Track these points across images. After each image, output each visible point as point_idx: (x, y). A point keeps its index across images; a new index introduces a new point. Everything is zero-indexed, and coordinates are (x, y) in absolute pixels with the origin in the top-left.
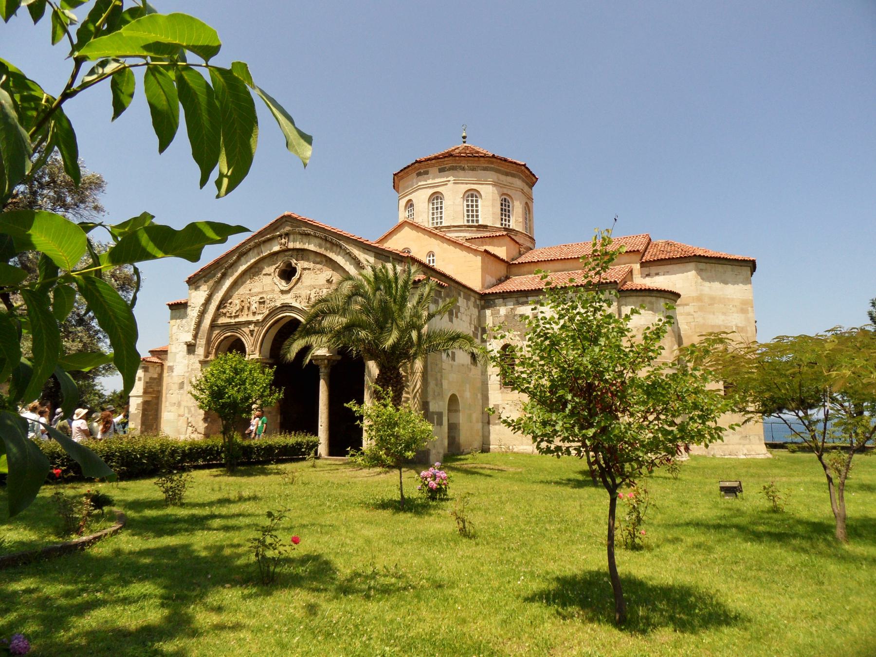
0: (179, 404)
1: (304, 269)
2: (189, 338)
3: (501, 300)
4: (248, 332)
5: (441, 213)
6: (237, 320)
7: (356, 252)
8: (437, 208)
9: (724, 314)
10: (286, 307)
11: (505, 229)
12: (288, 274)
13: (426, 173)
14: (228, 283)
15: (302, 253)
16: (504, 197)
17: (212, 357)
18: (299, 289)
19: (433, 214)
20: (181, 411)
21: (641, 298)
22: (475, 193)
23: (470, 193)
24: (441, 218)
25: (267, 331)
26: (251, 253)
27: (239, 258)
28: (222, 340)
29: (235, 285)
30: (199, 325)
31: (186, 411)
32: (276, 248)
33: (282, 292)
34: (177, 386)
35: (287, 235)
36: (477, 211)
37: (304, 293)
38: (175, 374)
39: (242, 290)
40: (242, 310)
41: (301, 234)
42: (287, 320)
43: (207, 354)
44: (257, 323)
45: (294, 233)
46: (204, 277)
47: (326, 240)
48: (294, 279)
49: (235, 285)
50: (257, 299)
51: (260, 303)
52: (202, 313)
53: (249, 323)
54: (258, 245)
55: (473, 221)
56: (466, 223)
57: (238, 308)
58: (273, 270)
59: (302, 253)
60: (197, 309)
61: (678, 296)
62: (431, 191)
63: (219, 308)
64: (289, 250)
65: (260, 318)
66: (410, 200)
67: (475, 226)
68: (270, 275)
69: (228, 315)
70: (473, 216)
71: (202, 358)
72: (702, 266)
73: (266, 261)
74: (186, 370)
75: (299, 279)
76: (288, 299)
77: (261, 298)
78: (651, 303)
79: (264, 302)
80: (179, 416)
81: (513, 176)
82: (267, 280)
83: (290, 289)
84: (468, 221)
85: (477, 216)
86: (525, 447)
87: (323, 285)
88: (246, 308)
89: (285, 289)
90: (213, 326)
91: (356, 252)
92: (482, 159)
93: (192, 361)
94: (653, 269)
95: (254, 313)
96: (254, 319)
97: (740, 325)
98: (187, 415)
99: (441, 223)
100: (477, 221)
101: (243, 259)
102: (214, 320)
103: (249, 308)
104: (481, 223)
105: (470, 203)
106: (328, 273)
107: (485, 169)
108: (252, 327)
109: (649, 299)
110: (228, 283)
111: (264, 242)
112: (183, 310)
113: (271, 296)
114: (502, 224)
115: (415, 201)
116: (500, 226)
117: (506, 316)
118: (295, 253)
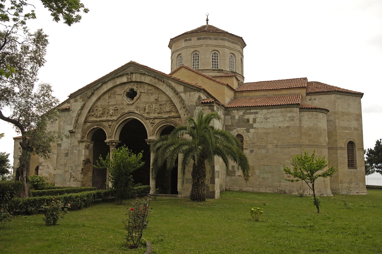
0: (65, 165)
1: (141, 93)
2: (71, 128)
3: (236, 111)
4: (107, 126)
5: (198, 62)
6: (101, 119)
7: (173, 84)
8: (196, 60)
9: (348, 121)
11: (232, 72)
12: (132, 94)
13: (190, 40)
14: (94, 98)
16: (231, 55)
17: (86, 139)
18: (138, 103)
19: (194, 62)
20: (67, 169)
21: (311, 112)
22: (217, 52)
23: (214, 52)
24: (198, 65)
25: (119, 126)
26: (109, 82)
27: (102, 85)
28: (91, 130)
30: (77, 121)
31: (70, 169)
34: (63, 155)
36: (217, 62)
37: (142, 106)
38: (62, 148)
40: (103, 114)
41: (140, 74)
42: (131, 120)
43: (83, 137)
44: (112, 121)
45: (135, 73)
46: (80, 94)
47: (155, 78)
48: (135, 98)
50: (113, 108)
51: (115, 110)
52: (79, 115)
53: (109, 121)
54: (113, 79)
55: (215, 67)
56: (212, 69)
57: (101, 112)
58: (123, 92)
60: (77, 112)
61: (328, 111)
62: (193, 50)
63: (89, 112)
64: (132, 82)
65: (115, 118)
66: (180, 54)
67: (216, 70)
68: (121, 95)
69: (95, 116)
70: (215, 65)
71: (80, 139)
72: (338, 96)
73: (118, 87)
74: (70, 146)
75: (138, 98)
76: (132, 108)
77: (115, 107)
78: (316, 115)
80: (65, 171)
81: (236, 43)
82: (119, 98)
83: (133, 103)
84: (213, 67)
85: (217, 65)
86: (249, 188)
87: (153, 102)
88: (106, 113)
89: (130, 103)
90: (85, 122)
91: (173, 84)
92: (221, 34)
93: (73, 141)
94: (313, 97)
95: (111, 115)
96: (112, 119)
97: (356, 127)
98: (70, 171)
99: (198, 67)
100: (218, 67)
101: (104, 86)
102: (86, 119)
103: (108, 113)
104: (219, 68)
105: (214, 58)
107: (222, 39)
108: (110, 123)
109: (315, 113)
110: (94, 98)
111: (118, 77)
113: (122, 107)
114: (230, 69)
115: (183, 55)
116: (229, 70)
117: (238, 119)
118: (136, 84)
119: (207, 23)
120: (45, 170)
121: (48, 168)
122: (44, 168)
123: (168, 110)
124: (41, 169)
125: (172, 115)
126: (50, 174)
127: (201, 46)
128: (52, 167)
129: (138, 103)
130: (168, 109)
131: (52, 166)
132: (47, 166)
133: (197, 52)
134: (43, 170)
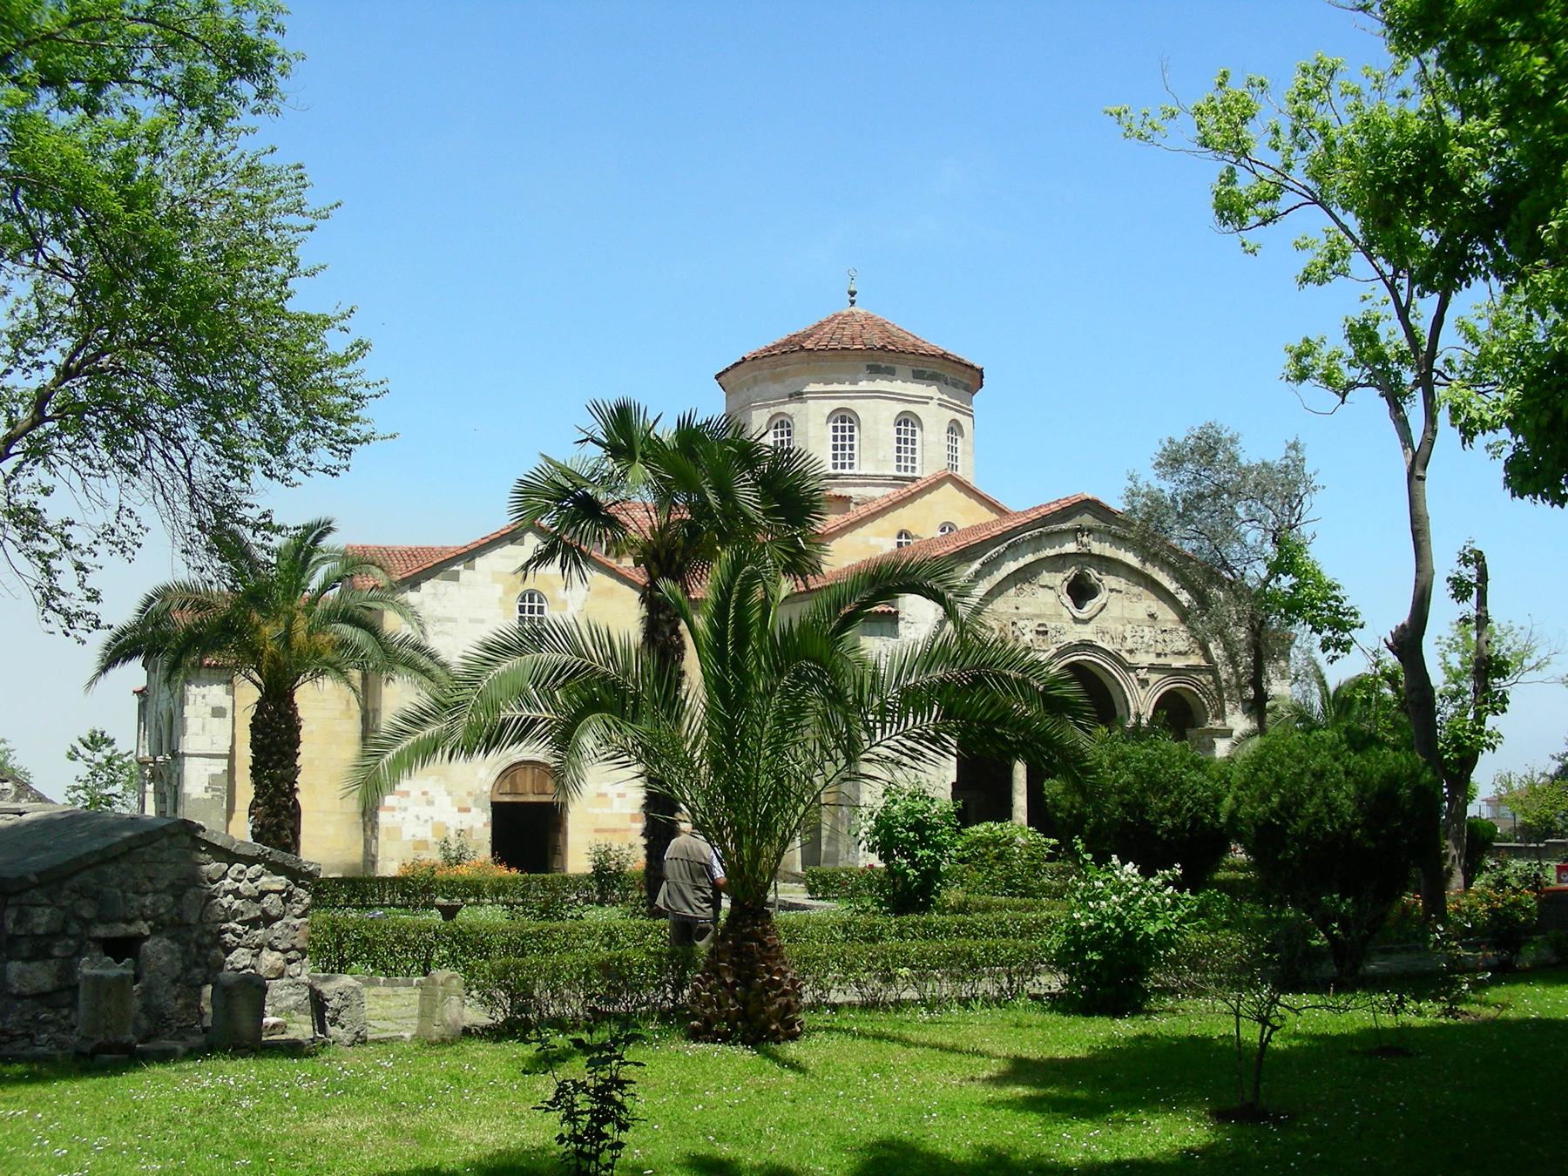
5: (913, 451)
10: (1086, 645)
12: (1081, 591)
15: (1110, 565)
18: (1105, 620)
29: (992, 594)
32: (1071, 547)
33: (1076, 620)
35: (1090, 531)
39: (1001, 605)
49: (992, 594)
50: (1033, 625)
59: (1110, 565)
64: (1090, 554)
76: (1087, 633)
79: (1046, 633)
82: (1049, 596)
106: (1151, 603)
112: (887, 625)
119: (853, 303)
120: (413, 810)
121: (430, 803)
122: (405, 802)
123: (1182, 649)
124: (392, 809)
125: (1190, 663)
126: (440, 827)
127: (925, 400)
128: (448, 800)
129: (1105, 620)
130: (1181, 645)
131: (449, 793)
132: (424, 793)
133: (911, 419)
134: (405, 809)
